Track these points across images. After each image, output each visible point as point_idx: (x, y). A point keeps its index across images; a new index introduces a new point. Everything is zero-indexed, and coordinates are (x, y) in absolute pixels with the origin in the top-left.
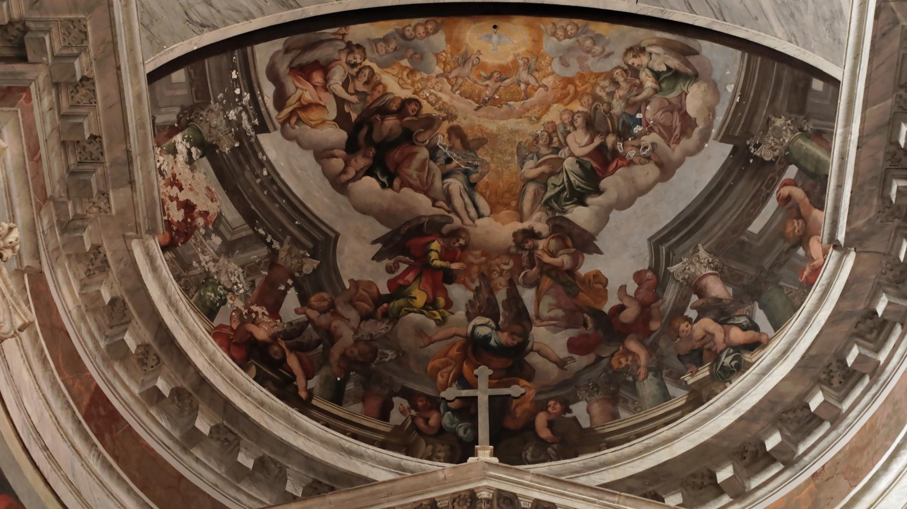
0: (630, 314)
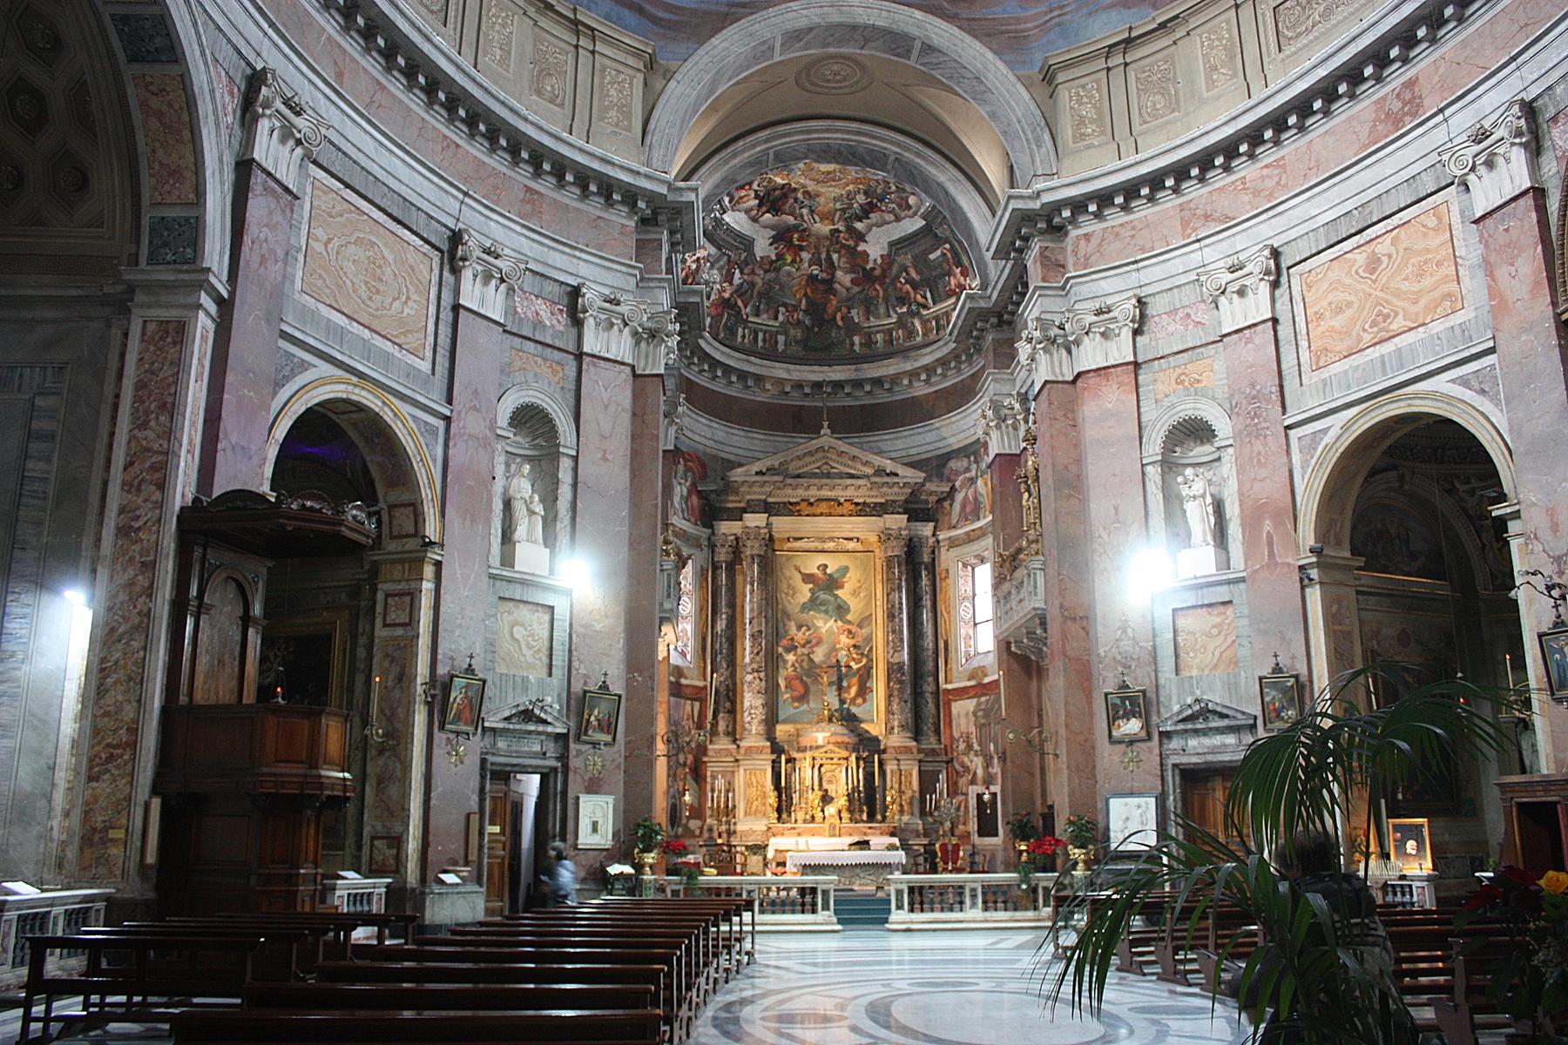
0: (877, 272)
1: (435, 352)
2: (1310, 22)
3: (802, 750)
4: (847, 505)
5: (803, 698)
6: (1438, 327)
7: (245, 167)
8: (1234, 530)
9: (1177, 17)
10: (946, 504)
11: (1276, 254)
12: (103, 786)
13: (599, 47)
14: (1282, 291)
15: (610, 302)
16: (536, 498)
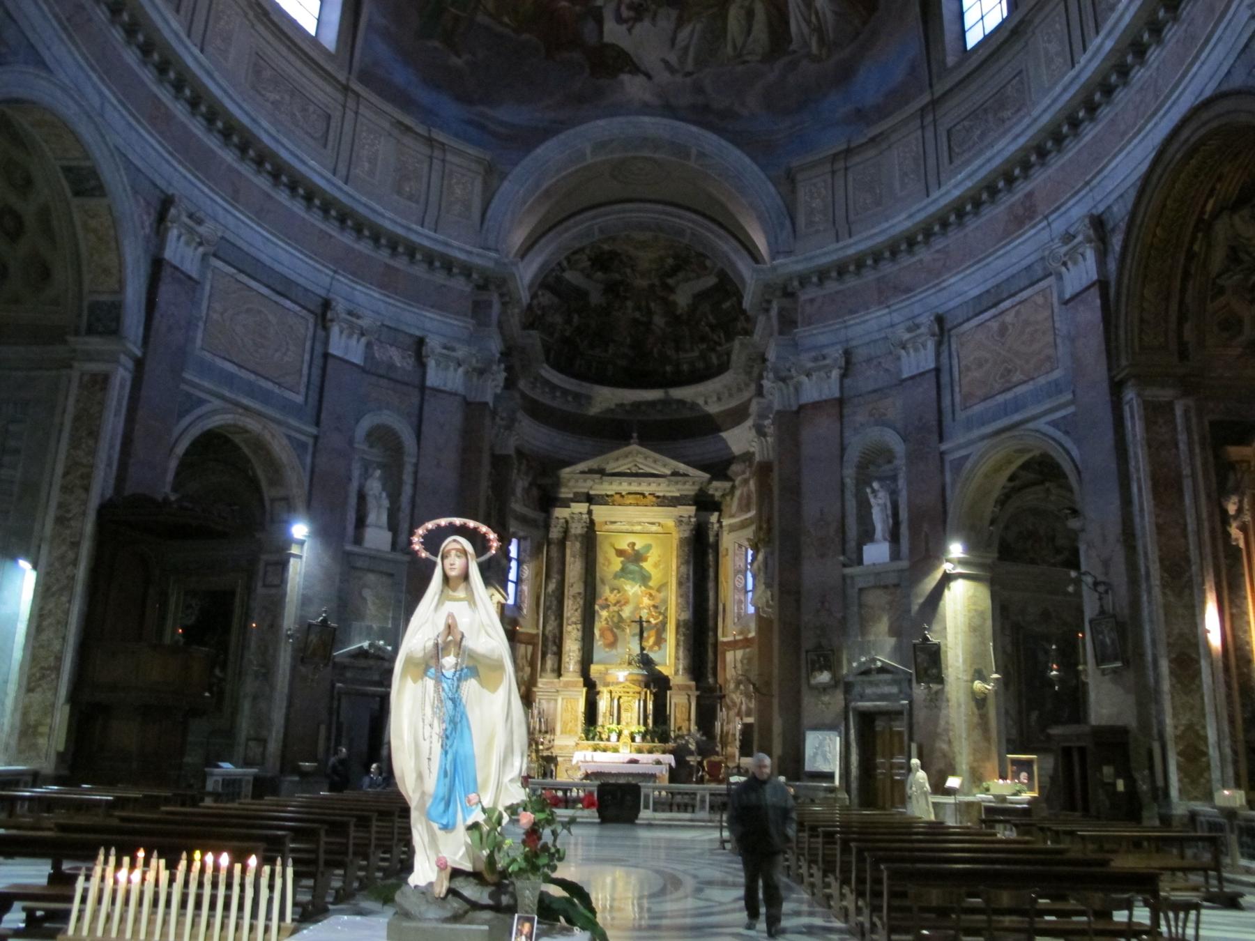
1: (308, 388)
2: (971, 143)
3: (607, 685)
4: (651, 497)
5: (613, 644)
6: (1042, 380)
7: (157, 265)
8: (904, 530)
9: (881, 134)
10: (728, 498)
11: (940, 320)
12: (37, 696)
13: (449, 157)
14: (945, 347)
15: (445, 347)
16: (384, 495)
